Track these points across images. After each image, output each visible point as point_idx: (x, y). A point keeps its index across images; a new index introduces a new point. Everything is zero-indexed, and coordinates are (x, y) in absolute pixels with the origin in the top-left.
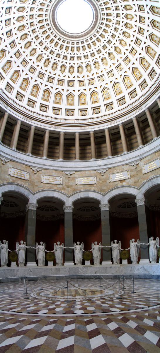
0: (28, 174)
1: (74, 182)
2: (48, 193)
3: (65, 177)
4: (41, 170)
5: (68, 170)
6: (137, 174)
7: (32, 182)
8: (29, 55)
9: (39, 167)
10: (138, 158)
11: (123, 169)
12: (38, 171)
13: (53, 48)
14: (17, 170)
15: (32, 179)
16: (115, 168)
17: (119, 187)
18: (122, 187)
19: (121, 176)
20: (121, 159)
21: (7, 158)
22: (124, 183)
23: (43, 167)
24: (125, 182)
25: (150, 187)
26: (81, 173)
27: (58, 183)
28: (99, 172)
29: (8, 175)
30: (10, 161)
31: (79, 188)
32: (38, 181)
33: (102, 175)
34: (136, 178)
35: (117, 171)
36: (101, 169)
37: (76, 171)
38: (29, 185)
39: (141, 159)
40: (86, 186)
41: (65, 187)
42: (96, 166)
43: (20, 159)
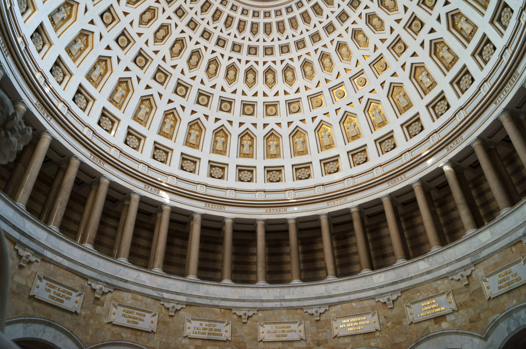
0: (228, 328)
1: (329, 331)
3: (309, 321)
4: (256, 312)
5: (313, 305)
6: (473, 300)
7: (239, 343)
8: (186, 70)
9: (251, 308)
10: (468, 261)
11: (437, 290)
12: (249, 317)
13: (235, 36)
14: (204, 323)
15: (239, 336)
16: (416, 289)
17: (433, 336)
18: (441, 334)
19: (433, 306)
20: (427, 266)
21: (178, 301)
22: (444, 325)
23: (258, 305)
24: (446, 321)
25: (514, 333)
26: (342, 307)
27: (295, 336)
28: (382, 300)
30: (186, 305)
31: (343, 344)
32: (253, 339)
33: (389, 307)
34: (471, 310)
35: (421, 294)
36: (385, 293)
37: (331, 305)
39: (475, 264)
40: (357, 338)
41: (310, 346)
42: (373, 289)
43: (207, 298)
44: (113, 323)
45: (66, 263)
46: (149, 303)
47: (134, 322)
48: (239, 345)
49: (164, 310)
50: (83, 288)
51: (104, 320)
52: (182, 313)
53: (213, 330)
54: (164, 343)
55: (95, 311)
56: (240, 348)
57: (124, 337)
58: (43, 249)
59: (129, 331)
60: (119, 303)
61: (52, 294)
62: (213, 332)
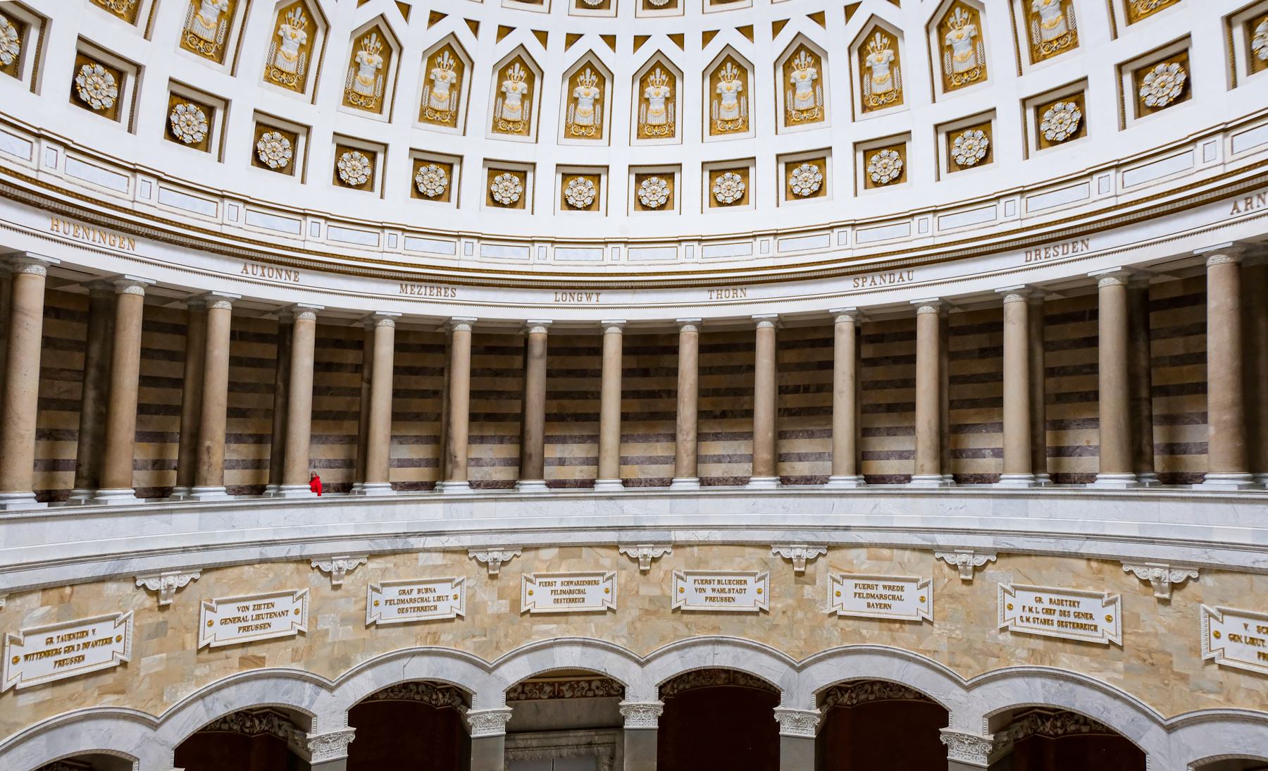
2: (1260, 735)
7: (1150, 652)
14: (1046, 597)
15: (1147, 634)
29: (1004, 630)
32: (1191, 649)
38: (1128, 670)
45: (717, 536)
46: (909, 560)
49: (946, 569)
50: (765, 563)
52: (991, 572)
53: (1072, 614)
54: (960, 640)
57: (867, 637)
58: (667, 533)
61: (710, 594)
62: (1072, 619)
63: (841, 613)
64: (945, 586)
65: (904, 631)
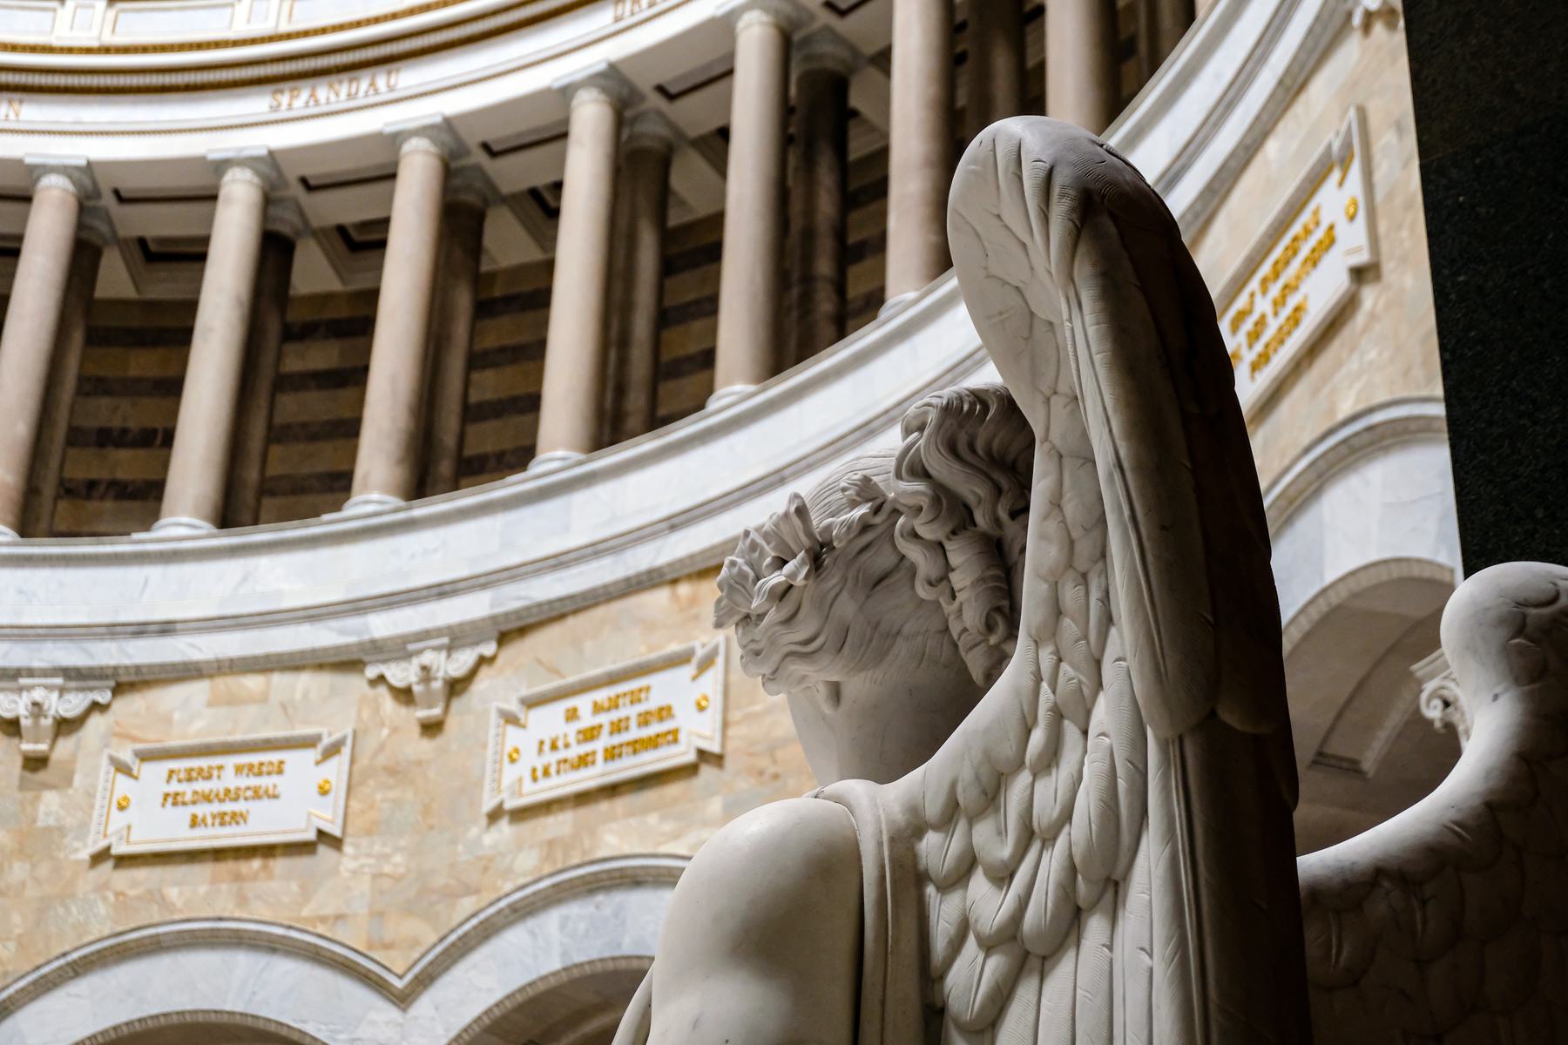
14: (583, 703)
29: (495, 816)
44: (114, 851)
46: (306, 695)
47: (223, 819)
48: (775, 762)
49: (388, 703)
51: (76, 850)
54: (398, 879)
55: (34, 821)
56: (776, 777)
59: (201, 872)
60: (139, 746)
62: (635, 733)
63: (119, 849)
64: (382, 747)
65: (270, 876)
